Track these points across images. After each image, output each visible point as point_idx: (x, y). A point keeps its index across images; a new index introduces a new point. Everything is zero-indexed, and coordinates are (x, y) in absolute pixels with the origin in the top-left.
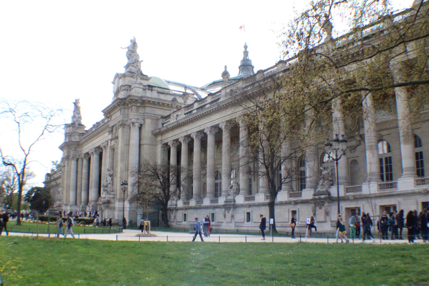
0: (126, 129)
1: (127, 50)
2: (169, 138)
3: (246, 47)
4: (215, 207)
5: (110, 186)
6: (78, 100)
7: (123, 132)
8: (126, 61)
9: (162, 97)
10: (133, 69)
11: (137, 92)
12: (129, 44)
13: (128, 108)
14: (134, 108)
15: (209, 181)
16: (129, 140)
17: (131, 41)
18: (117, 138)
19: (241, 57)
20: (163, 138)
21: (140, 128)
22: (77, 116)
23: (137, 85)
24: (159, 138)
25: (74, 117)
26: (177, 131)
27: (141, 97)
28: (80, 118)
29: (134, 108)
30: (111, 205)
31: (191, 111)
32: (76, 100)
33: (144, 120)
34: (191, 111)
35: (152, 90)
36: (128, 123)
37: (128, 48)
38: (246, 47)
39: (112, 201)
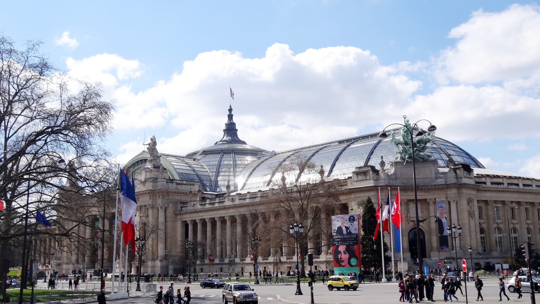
2: (188, 218)
3: (230, 110)
4: (222, 264)
7: (153, 212)
19: (226, 120)
20: (182, 217)
21: (165, 210)
24: (179, 217)
31: (205, 205)
33: (168, 204)
35: (172, 183)
37: (149, 144)
38: (230, 110)
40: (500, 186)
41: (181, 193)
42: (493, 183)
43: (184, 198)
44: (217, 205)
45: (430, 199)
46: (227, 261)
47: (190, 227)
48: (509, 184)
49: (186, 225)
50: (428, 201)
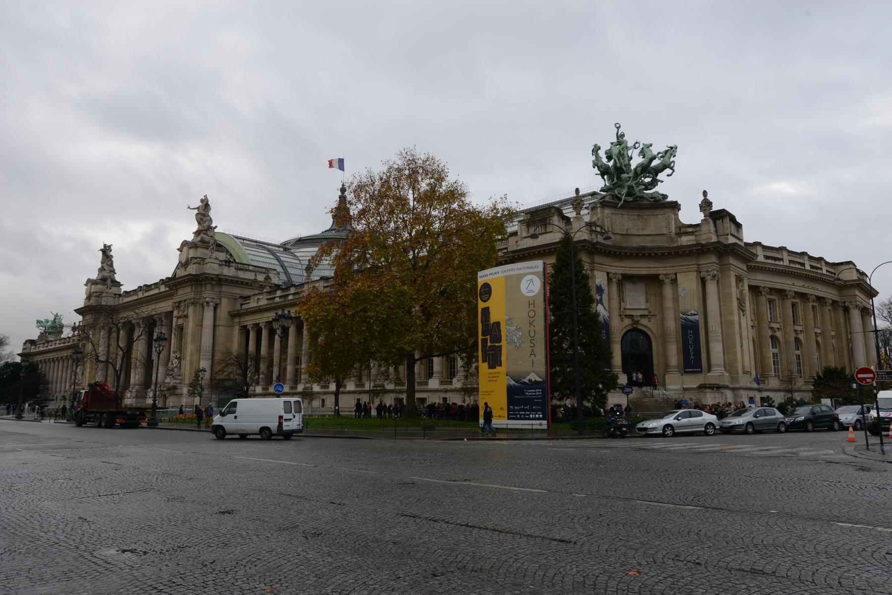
0: (199, 308)
1: (196, 211)
2: (249, 321)
5: (176, 370)
6: (109, 246)
7: (194, 311)
8: (195, 227)
9: (241, 275)
10: (207, 238)
11: (212, 269)
12: (199, 204)
13: (201, 285)
14: (209, 286)
15: (290, 368)
16: (202, 319)
17: (202, 201)
18: (186, 316)
21: (215, 308)
22: (107, 268)
23: (212, 261)
24: (237, 320)
25: (101, 270)
26: (258, 316)
27: (217, 275)
28: (113, 272)
29: (209, 286)
30: (178, 391)
31: (274, 298)
32: (105, 246)
33: (220, 299)
34: (274, 298)
35: (229, 266)
36: (201, 302)
37: (198, 208)
39: (179, 386)
40: (777, 263)
41: (242, 283)
42: (767, 257)
43: (247, 292)
44: (291, 297)
45: (666, 275)
46: (300, 388)
47: (252, 335)
48: (790, 261)
49: (245, 331)
50: (660, 277)
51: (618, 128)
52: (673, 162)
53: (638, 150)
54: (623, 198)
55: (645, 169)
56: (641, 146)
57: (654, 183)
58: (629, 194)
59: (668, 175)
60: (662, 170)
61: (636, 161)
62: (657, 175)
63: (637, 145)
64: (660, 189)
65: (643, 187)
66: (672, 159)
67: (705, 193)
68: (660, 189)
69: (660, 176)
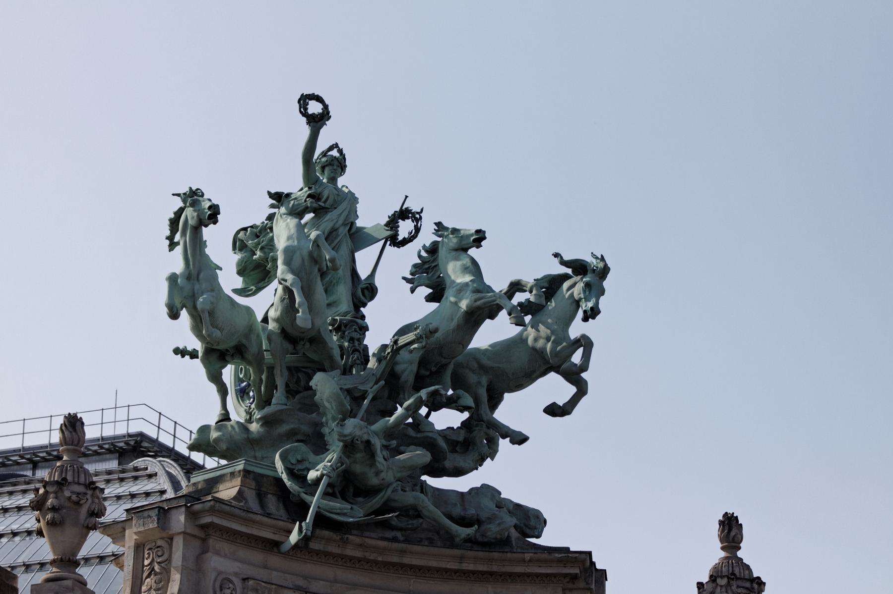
51: (317, 122)
52: (585, 343)
53: (410, 255)
54: (315, 501)
55: (438, 362)
56: (427, 237)
57: (479, 440)
58: (345, 485)
59: (553, 410)
60: (521, 380)
61: (395, 311)
62: (495, 401)
63: (405, 228)
64: (504, 474)
65: (417, 455)
66: (577, 328)
67: (730, 530)
68: (504, 474)
69: (516, 409)
